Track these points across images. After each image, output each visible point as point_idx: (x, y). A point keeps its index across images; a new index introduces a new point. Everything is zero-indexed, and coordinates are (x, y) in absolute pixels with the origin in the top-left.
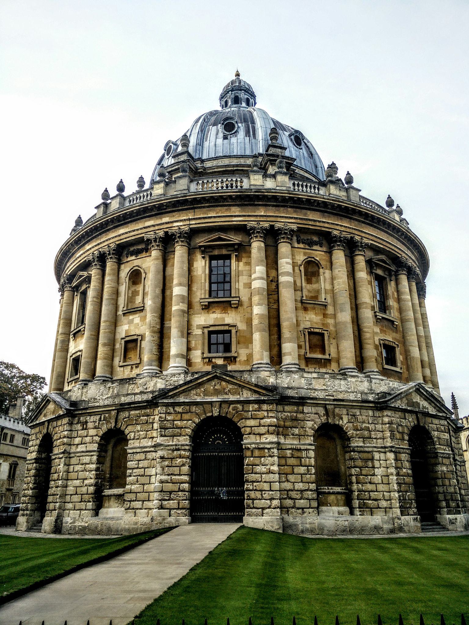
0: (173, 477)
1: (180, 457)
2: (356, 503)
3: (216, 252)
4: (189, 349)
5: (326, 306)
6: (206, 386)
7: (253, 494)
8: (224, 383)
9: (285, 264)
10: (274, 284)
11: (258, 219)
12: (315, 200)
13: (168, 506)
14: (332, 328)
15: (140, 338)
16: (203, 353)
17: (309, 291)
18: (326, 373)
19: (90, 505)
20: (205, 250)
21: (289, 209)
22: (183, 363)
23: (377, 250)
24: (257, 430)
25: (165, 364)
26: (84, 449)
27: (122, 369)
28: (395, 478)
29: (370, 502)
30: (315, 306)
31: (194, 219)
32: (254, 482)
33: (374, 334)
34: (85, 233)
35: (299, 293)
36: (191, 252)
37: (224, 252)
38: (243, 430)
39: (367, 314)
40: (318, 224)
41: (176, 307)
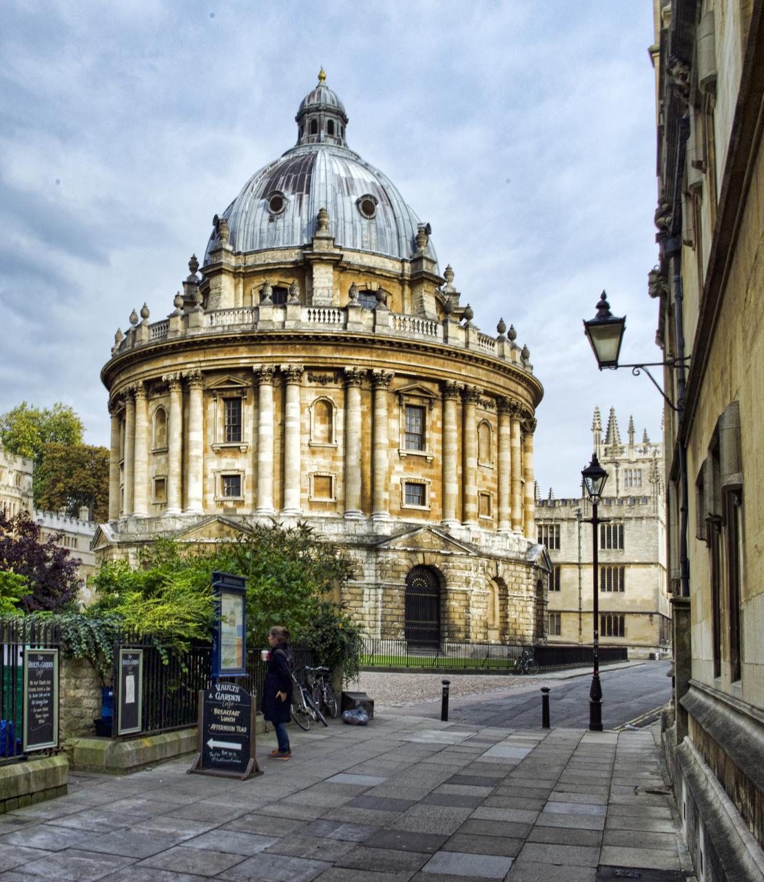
3: (228, 395)
5: (336, 448)
11: (265, 360)
31: (204, 361)
35: (307, 437)
37: (235, 394)
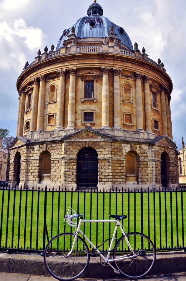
2: (140, 180)
3: (88, 79)
4: (76, 119)
7: (101, 177)
9: (117, 85)
10: (112, 93)
12: (130, 58)
13: (68, 180)
14: (135, 113)
15: (55, 115)
16: (81, 121)
17: (126, 97)
18: (131, 131)
19: (37, 179)
20: (82, 78)
21: (119, 61)
22: (73, 125)
23: (154, 81)
24: (103, 153)
25: (65, 125)
26: (33, 158)
28: (155, 171)
29: (145, 180)
30: (129, 103)
31: (78, 64)
32: (102, 172)
33: (151, 116)
34: (29, 70)
35: (122, 97)
36: (77, 78)
37: (91, 79)
38: (98, 153)
39: (149, 108)
40: (131, 68)
41: (70, 102)
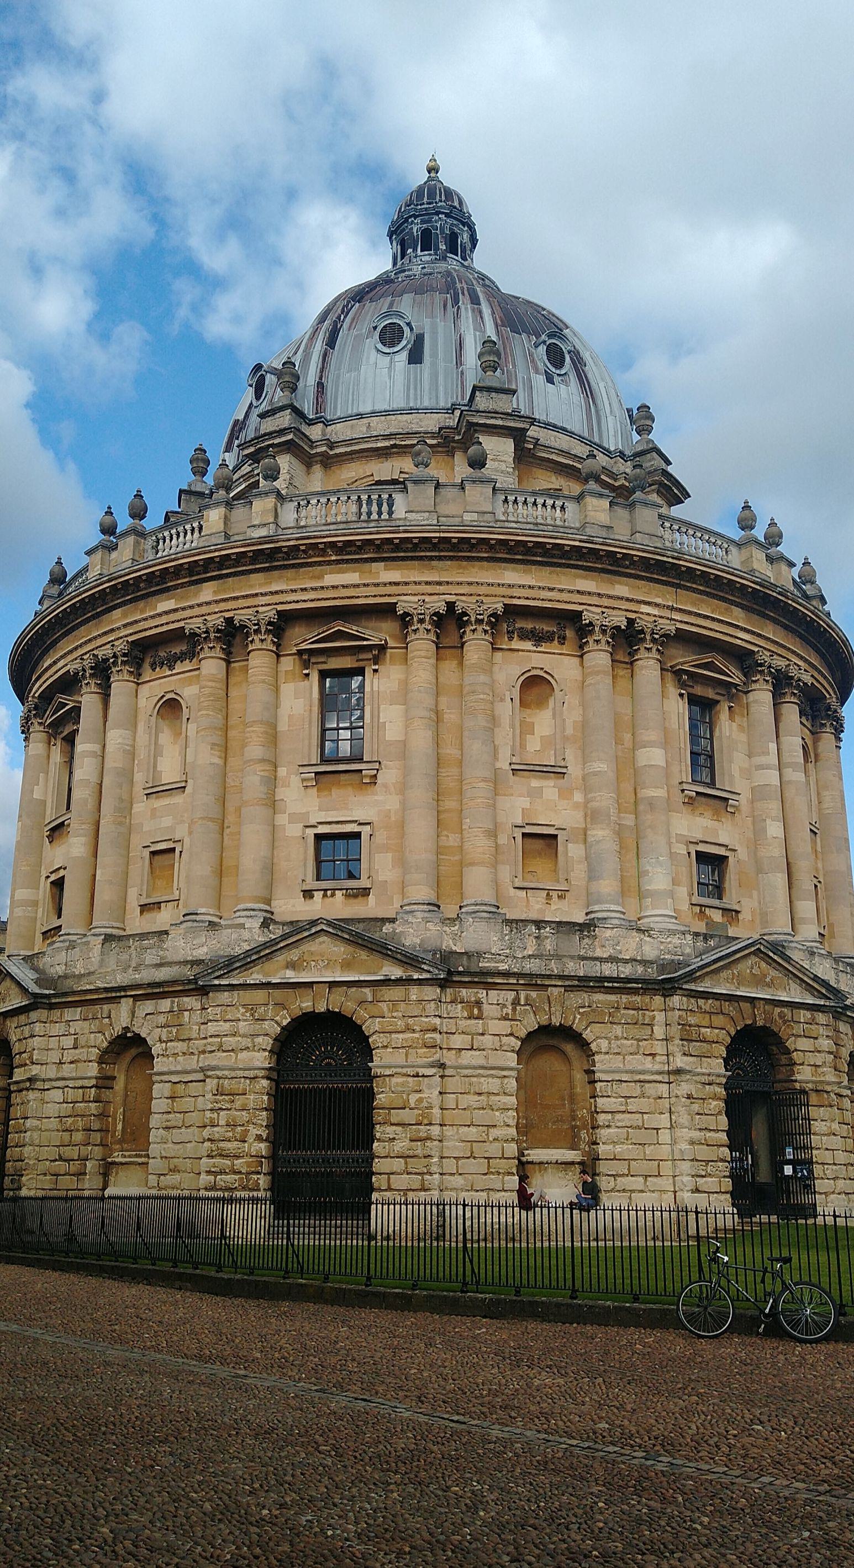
0: (709, 1134)
1: (715, 1097)
3: (699, 690)
6: (740, 966)
8: (763, 965)
27: (523, 894)
37: (710, 693)
